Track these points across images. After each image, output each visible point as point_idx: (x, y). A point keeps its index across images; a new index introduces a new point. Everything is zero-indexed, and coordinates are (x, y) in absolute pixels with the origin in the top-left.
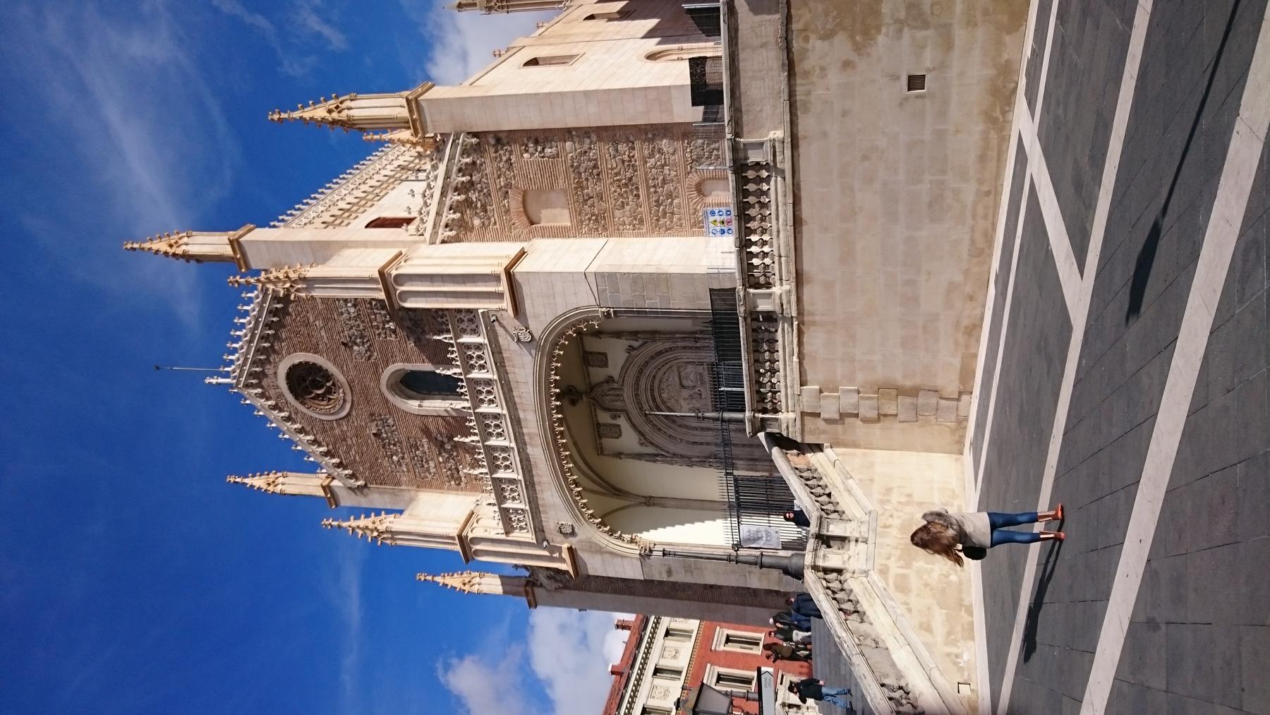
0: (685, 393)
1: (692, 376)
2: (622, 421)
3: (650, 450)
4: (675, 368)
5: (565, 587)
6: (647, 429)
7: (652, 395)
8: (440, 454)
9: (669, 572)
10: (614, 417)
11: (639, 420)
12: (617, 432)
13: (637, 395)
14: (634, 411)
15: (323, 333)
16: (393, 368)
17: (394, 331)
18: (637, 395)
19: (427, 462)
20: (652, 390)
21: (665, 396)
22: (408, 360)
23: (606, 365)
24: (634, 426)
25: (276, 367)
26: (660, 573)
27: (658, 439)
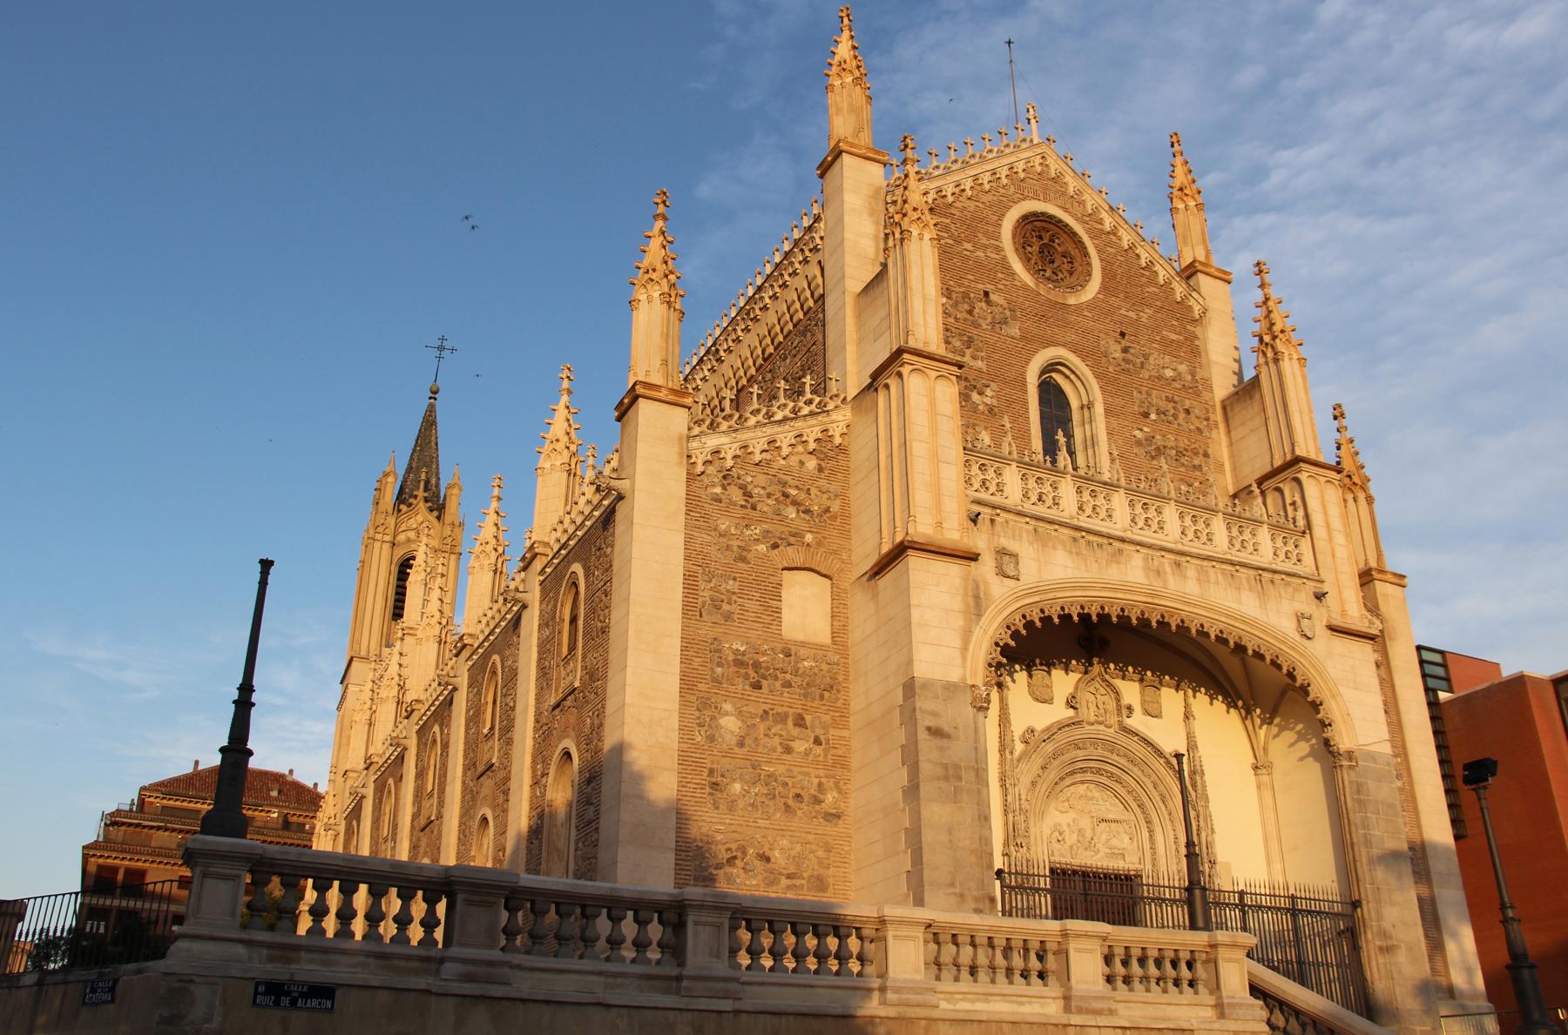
0: (1085, 823)
1: (1115, 842)
5: (692, 478)
6: (1049, 748)
9: (936, 732)
10: (1071, 703)
11: (1063, 737)
14: (1077, 733)
15: (1131, 314)
17: (1146, 415)
18: (1096, 741)
20: (1099, 771)
21: (1082, 788)
22: (1108, 412)
23: (1147, 713)
26: (934, 714)
27: (1037, 761)
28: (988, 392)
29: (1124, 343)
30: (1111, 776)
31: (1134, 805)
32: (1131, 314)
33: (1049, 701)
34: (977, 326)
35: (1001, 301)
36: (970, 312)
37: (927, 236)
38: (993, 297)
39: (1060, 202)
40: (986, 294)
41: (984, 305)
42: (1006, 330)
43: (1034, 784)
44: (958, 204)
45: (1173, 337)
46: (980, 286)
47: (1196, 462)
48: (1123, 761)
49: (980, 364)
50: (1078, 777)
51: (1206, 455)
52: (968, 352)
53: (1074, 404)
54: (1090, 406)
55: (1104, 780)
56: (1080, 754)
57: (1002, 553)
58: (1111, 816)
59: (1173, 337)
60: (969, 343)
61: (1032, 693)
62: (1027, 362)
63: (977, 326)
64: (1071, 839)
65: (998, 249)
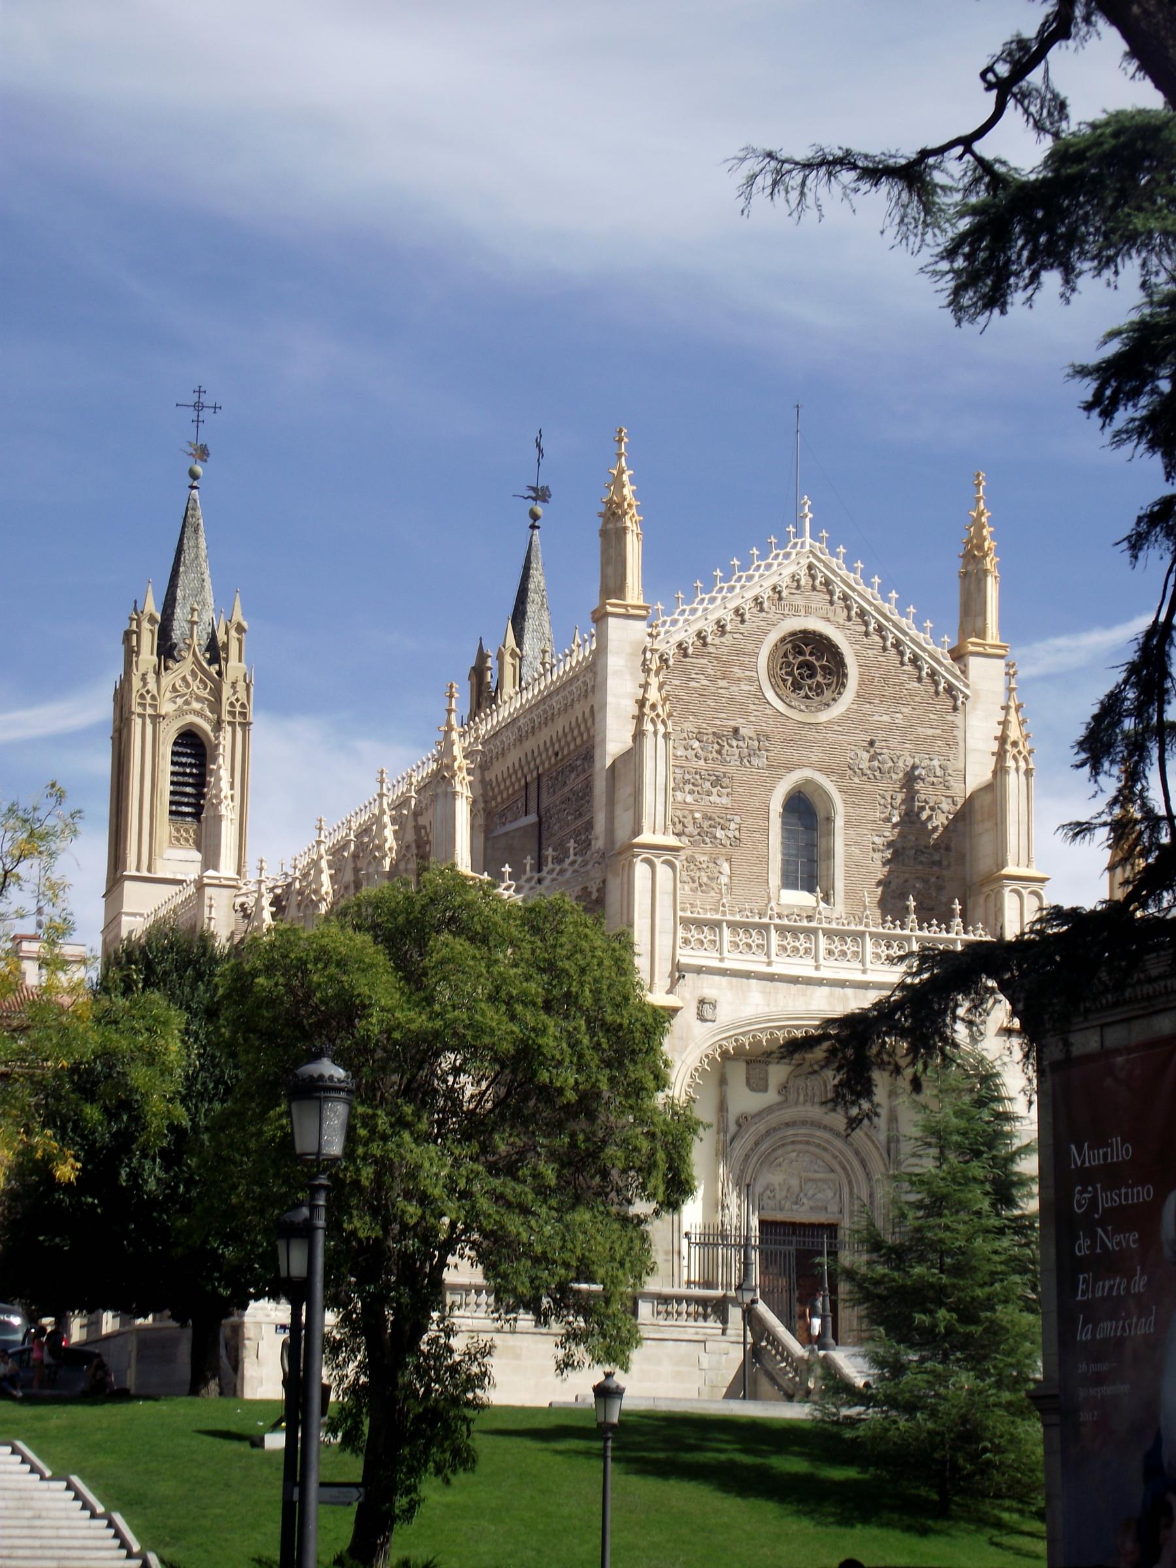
0: (794, 1182)
2: (771, 1097)
3: (733, 1128)
4: (832, 1175)
7: (800, 1142)
8: (706, 817)
10: (784, 1089)
11: (774, 1119)
12: (757, 1084)
13: (804, 1123)
15: (886, 718)
16: (837, 798)
18: (804, 1123)
19: (691, 792)
20: (808, 1143)
21: (794, 1155)
22: (848, 824)
24: (770, 1109)
25: (838, 626)
28: (733, 826)
29: (872, 750)
30: (819, 1146)
31: (837, 1168)
32: (886, 718)
33: (765, 1090)
34: (724, 762)
35: (754, 735)
36: (719, 752)
37: (661, 729)
38: (742, 731)
39: (822, 613)
40: (736, 731)
41: (734, 743)
42: (755, 761)
43: (747, 1157)
44: (717, 641)
45: (930, 732)
46: (733, 723)
47: (936, 857)
48: (827, 1135)
49: (724, 800)
50: (790, 1148)
51: (948, 849)
52: (714, 790)
53: (821, 815)
54: (829, 820)
55: (812, 1149)
56: (791, 1132)
57: (702, 1002)
58: (818, 1176)
59: (930, 732)
60: (717, 782)
61: (748, 1084)
62: (771, 791)
63: (724, 762)
64: (780, 1195)
65: (750, 680)
